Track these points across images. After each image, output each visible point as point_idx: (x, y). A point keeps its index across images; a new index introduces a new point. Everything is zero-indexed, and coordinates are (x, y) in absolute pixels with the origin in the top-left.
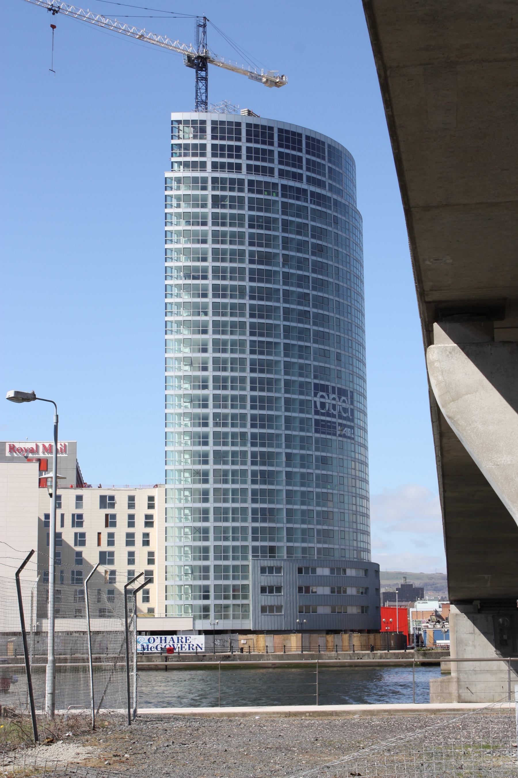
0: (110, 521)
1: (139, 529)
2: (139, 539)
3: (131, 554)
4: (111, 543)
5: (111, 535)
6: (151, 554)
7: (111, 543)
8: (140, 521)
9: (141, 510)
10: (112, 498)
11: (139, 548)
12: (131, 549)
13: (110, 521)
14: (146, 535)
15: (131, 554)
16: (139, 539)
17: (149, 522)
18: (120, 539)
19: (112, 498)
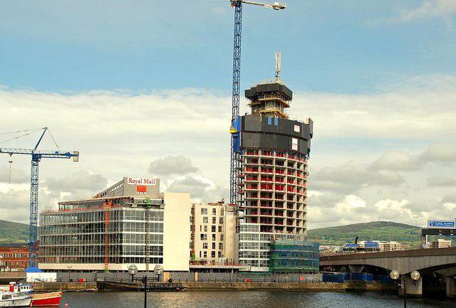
0: (206, 219)
1: (217, 224)
2: (217, 229)
3: (214, 236)
4: (206, 230)
5: (206, 227)
6: (222, 236)
7: (206, 230)
8: (218, 220)
9: (218, 217)
10: (206, 210)
11: (217, 233)
12: (213, 233)
13: (206, 219)
14: (220, 227)
15: (214, 236)
16: (217, 229)
17: (221, 221)
18: (210, 229)
19: (206, 210)
